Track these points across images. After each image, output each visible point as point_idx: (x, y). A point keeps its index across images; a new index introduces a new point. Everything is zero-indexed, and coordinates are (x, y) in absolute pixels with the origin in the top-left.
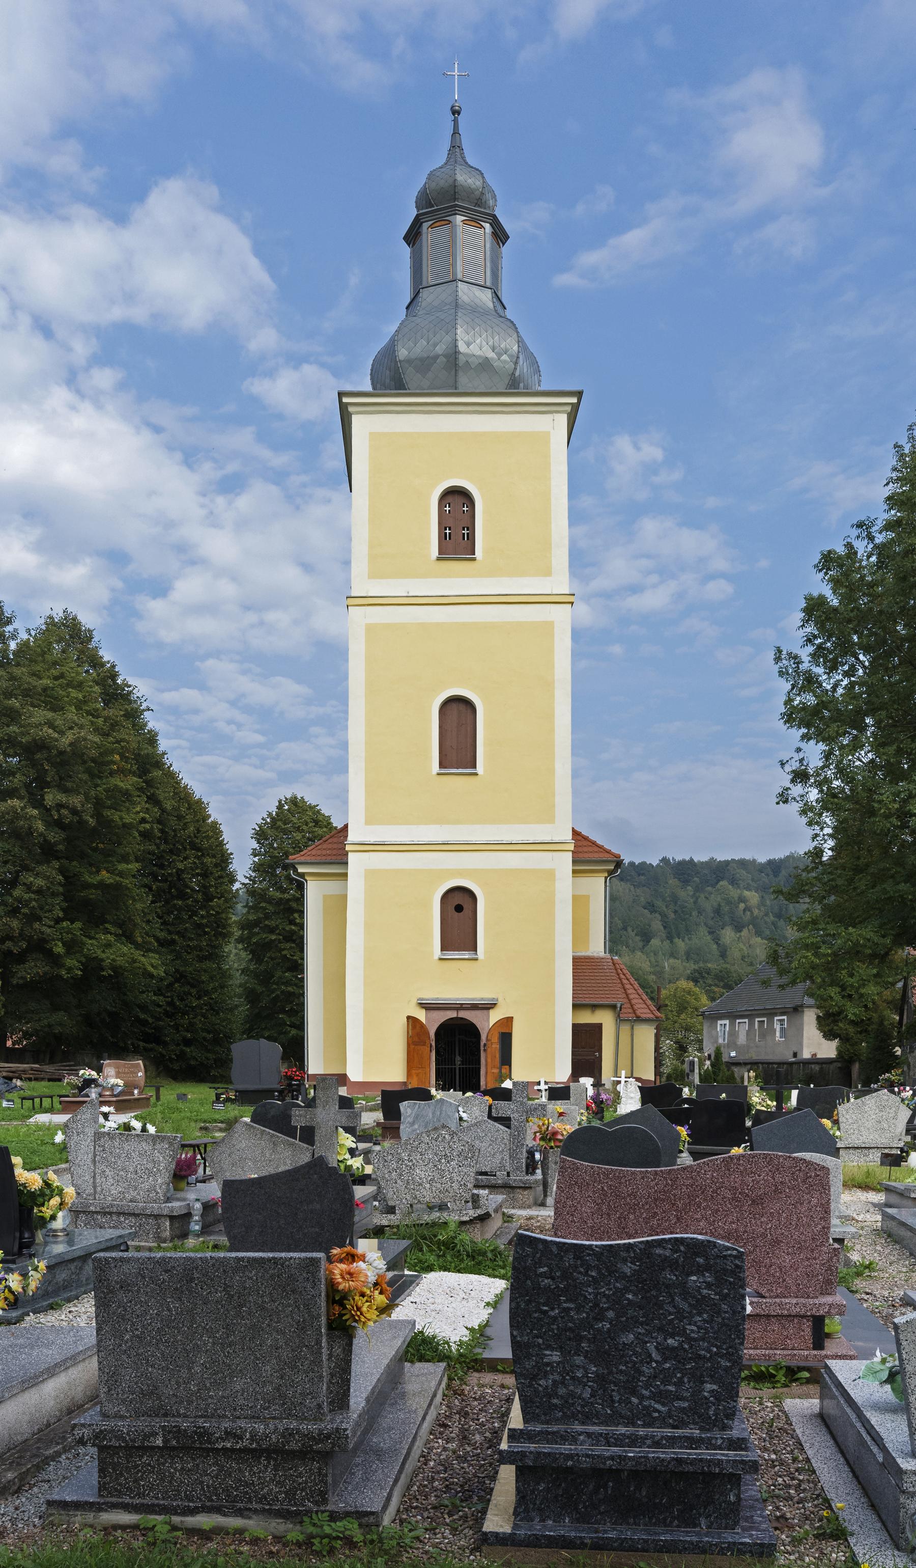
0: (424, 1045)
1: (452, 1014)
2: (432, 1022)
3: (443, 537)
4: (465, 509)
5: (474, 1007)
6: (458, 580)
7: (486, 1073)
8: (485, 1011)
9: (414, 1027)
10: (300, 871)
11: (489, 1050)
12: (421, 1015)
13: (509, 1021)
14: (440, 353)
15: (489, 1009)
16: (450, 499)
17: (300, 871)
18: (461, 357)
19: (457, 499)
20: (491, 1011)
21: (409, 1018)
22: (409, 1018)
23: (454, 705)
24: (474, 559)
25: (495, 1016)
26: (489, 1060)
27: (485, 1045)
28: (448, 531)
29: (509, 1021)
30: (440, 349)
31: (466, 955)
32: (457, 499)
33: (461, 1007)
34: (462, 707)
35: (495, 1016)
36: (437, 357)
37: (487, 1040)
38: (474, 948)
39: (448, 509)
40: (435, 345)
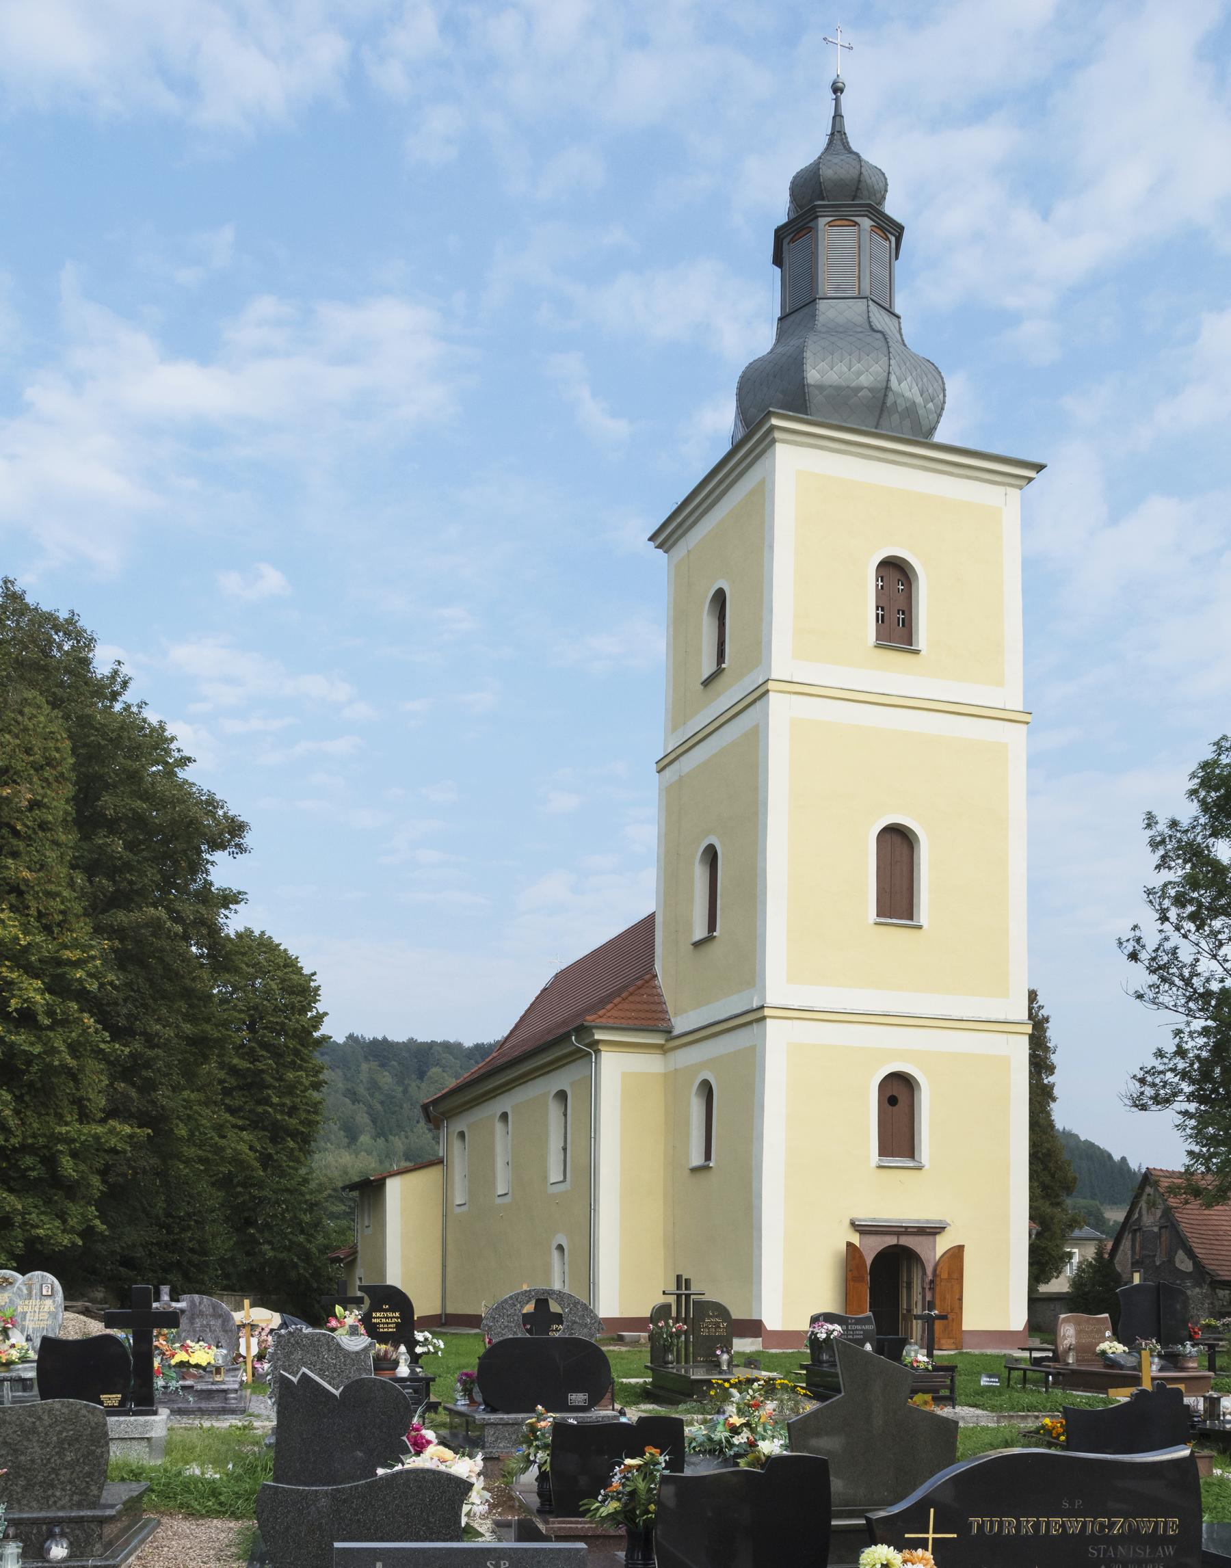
1: (891, 1241)
2: (871, 1248)
3: (881, 620)
6: (893, 674)
8: (931, 1238)
11: (938, 1289)
13: (961, 1248)
15: (935, 1234)
18: (890, 394)
19: (896, 574)
20: (938, 1238)
25: (943, 1245)
27: (932, 1282)
29: (961, 1248)
32: (896, 574)
35: (943, 1245)
36: (860, 389)
40: (859, 374)
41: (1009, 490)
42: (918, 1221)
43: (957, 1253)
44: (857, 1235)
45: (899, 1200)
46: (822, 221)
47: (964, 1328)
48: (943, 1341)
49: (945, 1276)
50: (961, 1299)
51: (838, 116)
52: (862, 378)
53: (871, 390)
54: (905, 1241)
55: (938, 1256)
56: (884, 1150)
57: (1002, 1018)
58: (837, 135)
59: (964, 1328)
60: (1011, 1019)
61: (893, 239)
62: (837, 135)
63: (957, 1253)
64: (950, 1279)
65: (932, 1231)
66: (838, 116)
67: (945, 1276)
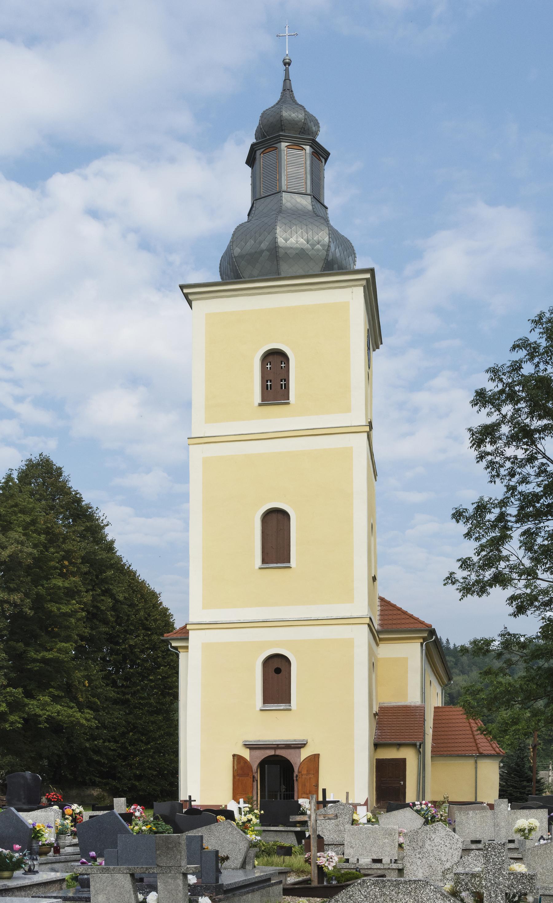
1: (271, 753)
4: (283, 365)
5: (288, 747)
6: (277, 419)
8: (297, 750)
9: (239, 763)
10: (173, 645)
11: (300, 780)
14: (265, 248)
15: (300, 748)
16: (271, 358)
17: (173, 645)
20: (302, 750)
23: (274, 515)
24: (288, 403)
25: (305, 754)
27: (297, 776)
28: (269, 383)
30: (264, 246)
31: (282, 706)
33: (277, 747)
34: (280, 516)
35: (305, 754)
36: (262, 251)
37: (299, 772)
38: (287, 700)
39: (269, 366)
40: (261, 243)
41: (355, 289)
42: (287, 741)
43: (315, 759)
45: (277, 728)
46: (258, 153)
49: (304, 772)
51: (287, 79)
52: (262, 245)
53: (267, 250)
54: (279, 752)
56: (266, 700)
57: (348, 615)
58: (287, 90)
60: (355, 615)
61: (308, 148)
62: (287, 90)
63: (315, 759)
64: (308, 773)
65: (301, 746)
66: (287, 79)
67: (304, 772)
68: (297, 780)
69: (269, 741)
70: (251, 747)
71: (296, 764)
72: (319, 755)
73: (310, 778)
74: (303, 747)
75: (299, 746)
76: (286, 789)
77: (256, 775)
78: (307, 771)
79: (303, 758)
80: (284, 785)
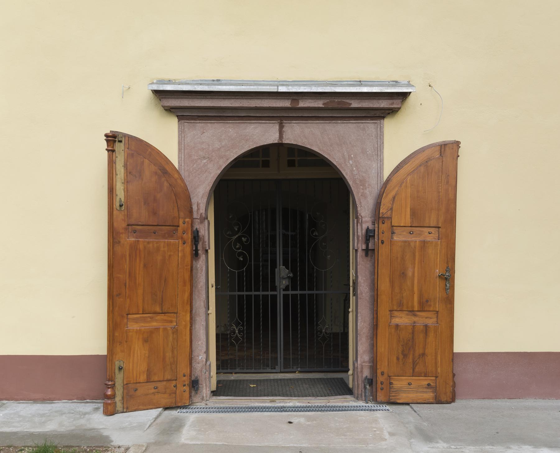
0: (171, 235)
1: (264, 134)
2: (198, 157)
7: (375, 326)
8: (370, 126)
11: (383, 251)
12: (165, 136)
13: (449, 151)
21: (112, 139)
22: (112, 139)
25: (401, 140)
26: (384, 285)
27: (369, 235)
29: (449, 151)
33: (293, 106)
35: (401, 140)
37: (377, 217)
43: (441, 162)
44: (172, 124)
47: (457, 349)
48: (399, 383)
49: (403, 218)
50: (448, 278)
54: (299, 134)
55: (386, 174)
59: (461, 345)
63: (441, 162)
64: (417, 220)
67: (403, 218)
68: (367, 252)
69: (256, 83)
70: (185, 105)
71: (363, 182)
72: (457, 144)
73: (424, 244)
74: (392, 112)
75: (384, 104)
76: (293, 280)
77: (203, 232)
78: (414, 213)
79: (392, 157)
80: (285, 264)
